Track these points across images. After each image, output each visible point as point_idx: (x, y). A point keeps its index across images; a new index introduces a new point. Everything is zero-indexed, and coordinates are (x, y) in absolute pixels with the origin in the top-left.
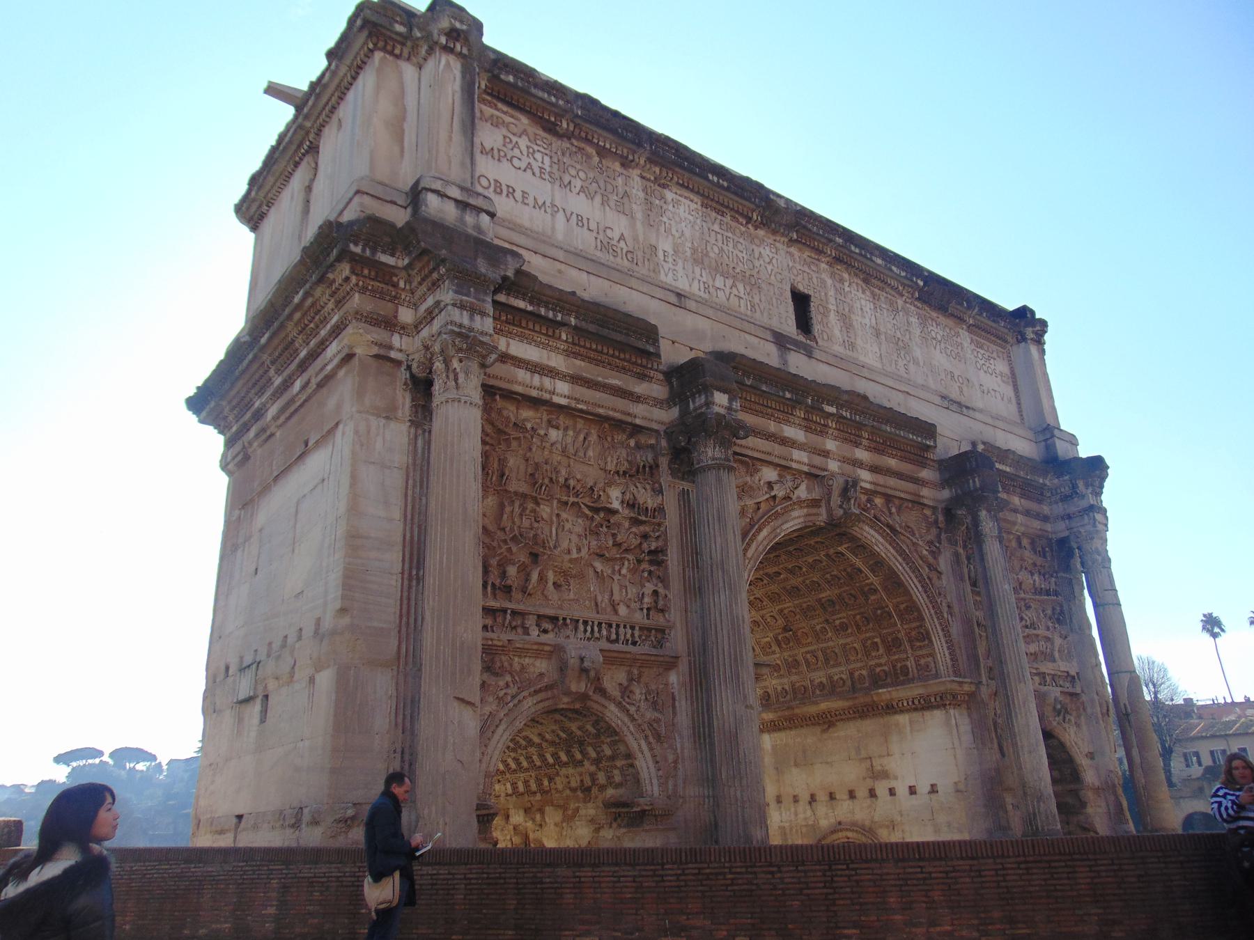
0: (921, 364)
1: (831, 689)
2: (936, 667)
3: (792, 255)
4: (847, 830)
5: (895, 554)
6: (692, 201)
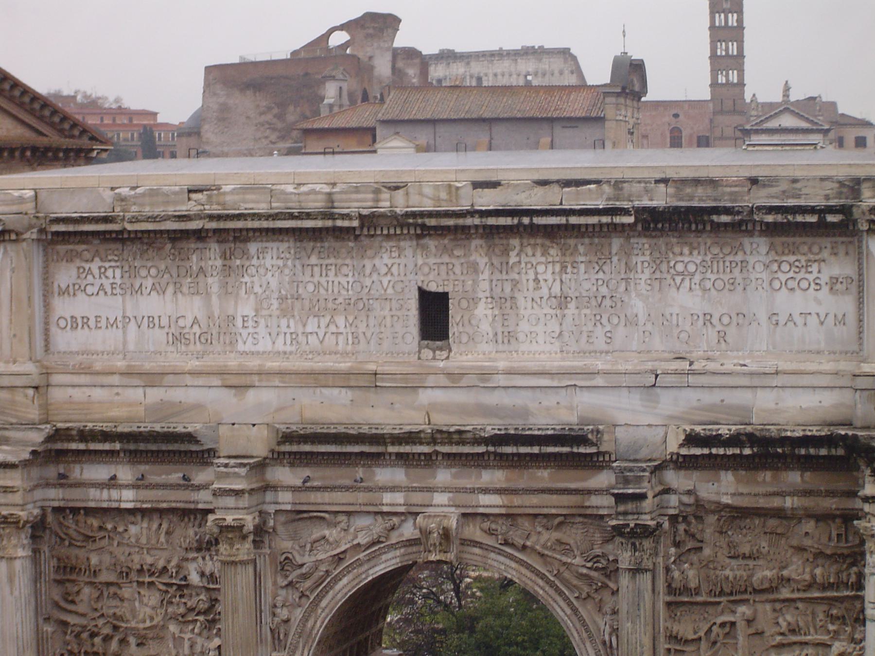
0: (642, 319)
3: (424, 248)
6: (282, 241)
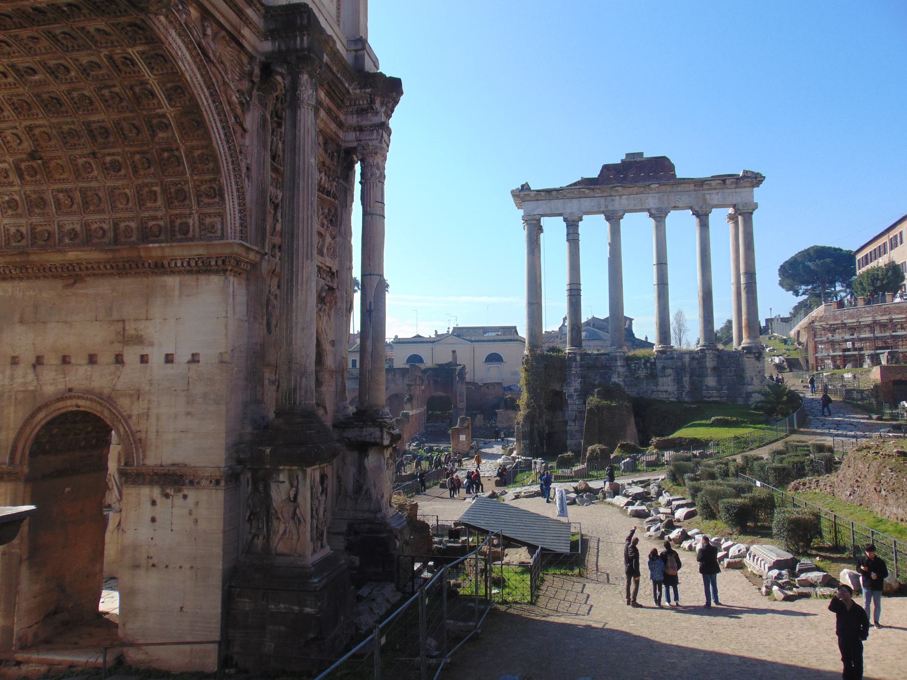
1: (86, 238)
2: (222, 229)
4: (79, 397)
5: (202, 83)
